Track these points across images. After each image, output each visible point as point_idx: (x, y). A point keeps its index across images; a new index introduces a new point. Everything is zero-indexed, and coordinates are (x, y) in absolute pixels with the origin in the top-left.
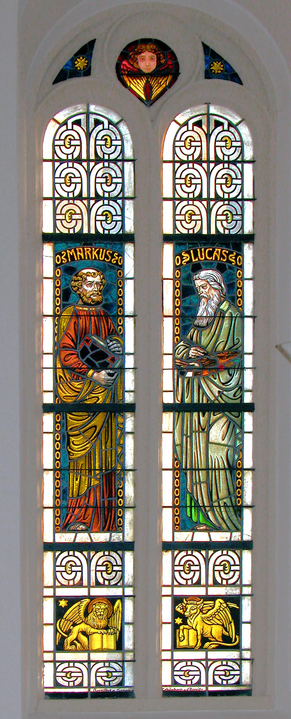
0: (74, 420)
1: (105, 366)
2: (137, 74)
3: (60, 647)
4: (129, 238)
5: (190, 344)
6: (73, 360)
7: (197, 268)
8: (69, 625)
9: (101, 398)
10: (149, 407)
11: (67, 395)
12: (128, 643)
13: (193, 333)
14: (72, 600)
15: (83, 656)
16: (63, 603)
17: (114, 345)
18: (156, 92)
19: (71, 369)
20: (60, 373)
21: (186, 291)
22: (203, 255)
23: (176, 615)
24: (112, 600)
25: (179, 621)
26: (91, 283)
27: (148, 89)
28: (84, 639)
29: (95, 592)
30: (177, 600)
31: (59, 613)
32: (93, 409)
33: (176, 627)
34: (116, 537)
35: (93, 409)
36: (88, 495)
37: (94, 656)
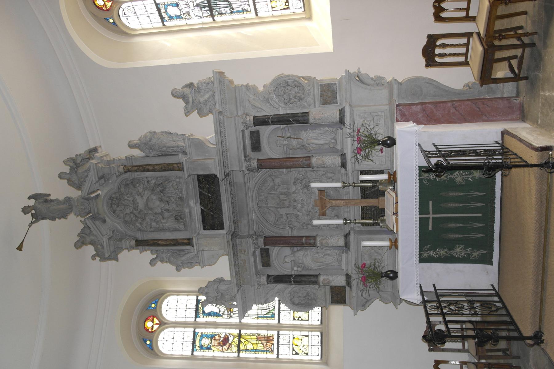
0: (242, 347)
1: (228, 338)
2: (153, 327)
3: (307, 354)
4: (194, 330)
5: (224, 314)
6: (226, 347)
7: (204, 312)
8: (301, 351)
9: (236, 340)
10: (241, 326)
11: (235, 349)
12: (306, 333)
13: (221, 313)
14: (294, 350)
15: (310, 347)
16: (294, 353)
17: (223, 335)
18: (158, 322)
19: (228, 348)
20: (229, 351)
21: (210, 314)
22: (200, 310)
23: (298, 320)
24: (294, 338)
25: (300, 319)
26: (206, 342)
27: (157, 324)
28: (304, 347)
29: (291, 343)
30: (294, 319)
31: (297, 354)
32: (240, 342)
33: (302, 320)
34: (276, 337)
35: (240, 342)
36: (263, 344)
37: (310, 344)
